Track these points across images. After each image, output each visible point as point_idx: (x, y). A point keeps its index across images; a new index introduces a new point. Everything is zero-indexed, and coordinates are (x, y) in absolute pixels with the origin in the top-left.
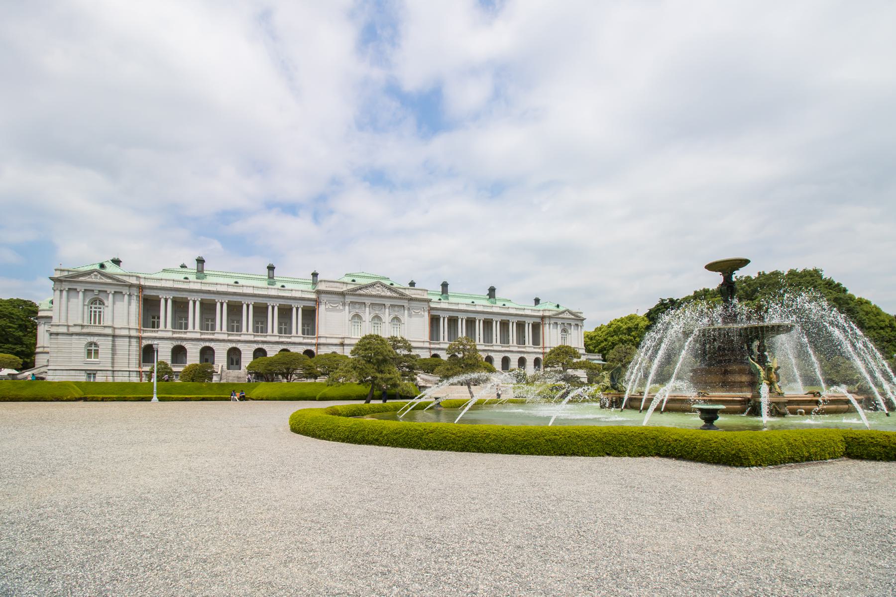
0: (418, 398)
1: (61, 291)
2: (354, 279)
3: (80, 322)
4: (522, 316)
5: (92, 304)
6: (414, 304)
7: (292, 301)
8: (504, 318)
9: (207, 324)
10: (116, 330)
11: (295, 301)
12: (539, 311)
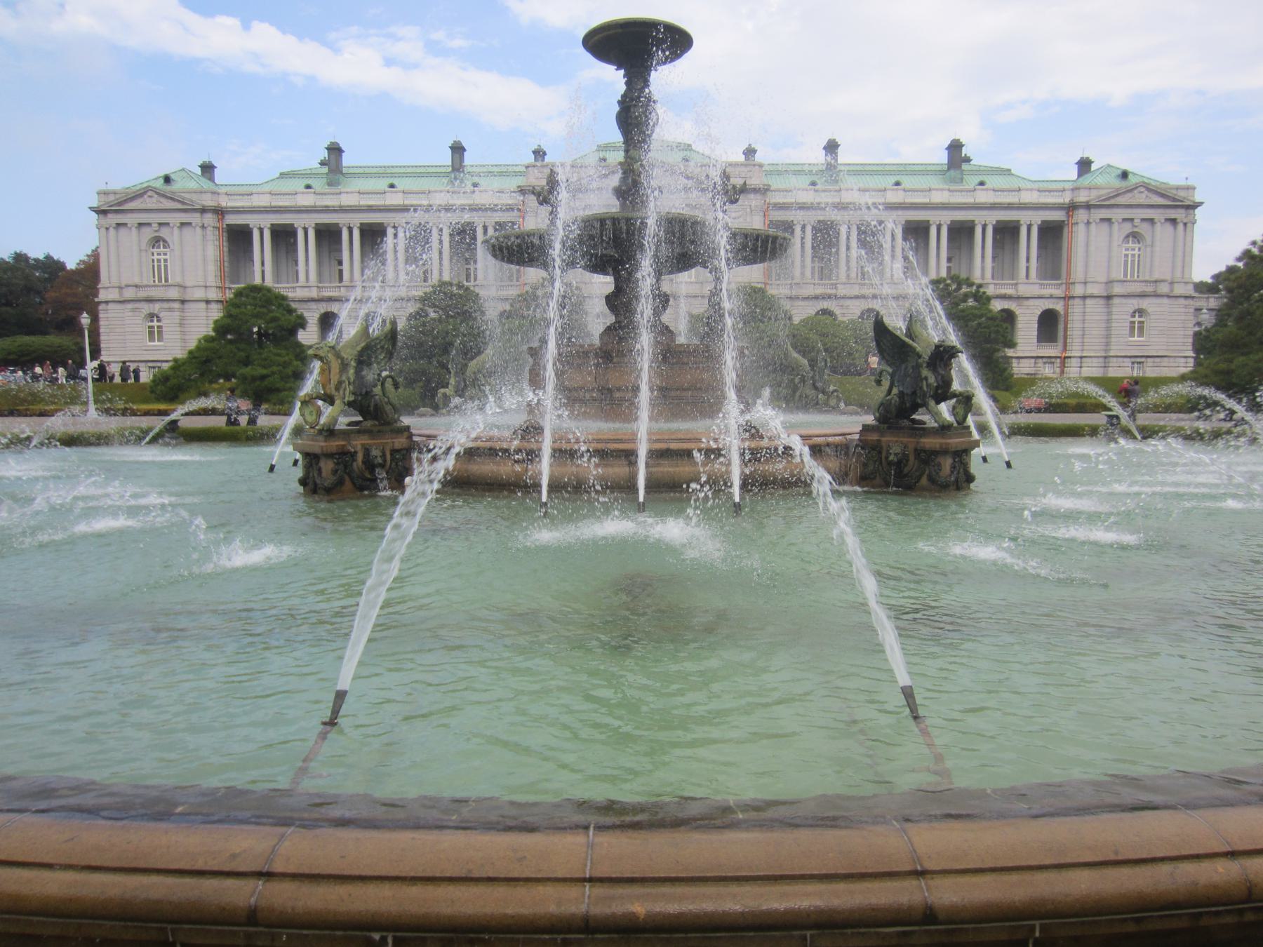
1: (107, 229)
3: (137, 281)
4: (1009, 207)
5: (153, 248)
10: (188, 290)
12: (1064, 190)
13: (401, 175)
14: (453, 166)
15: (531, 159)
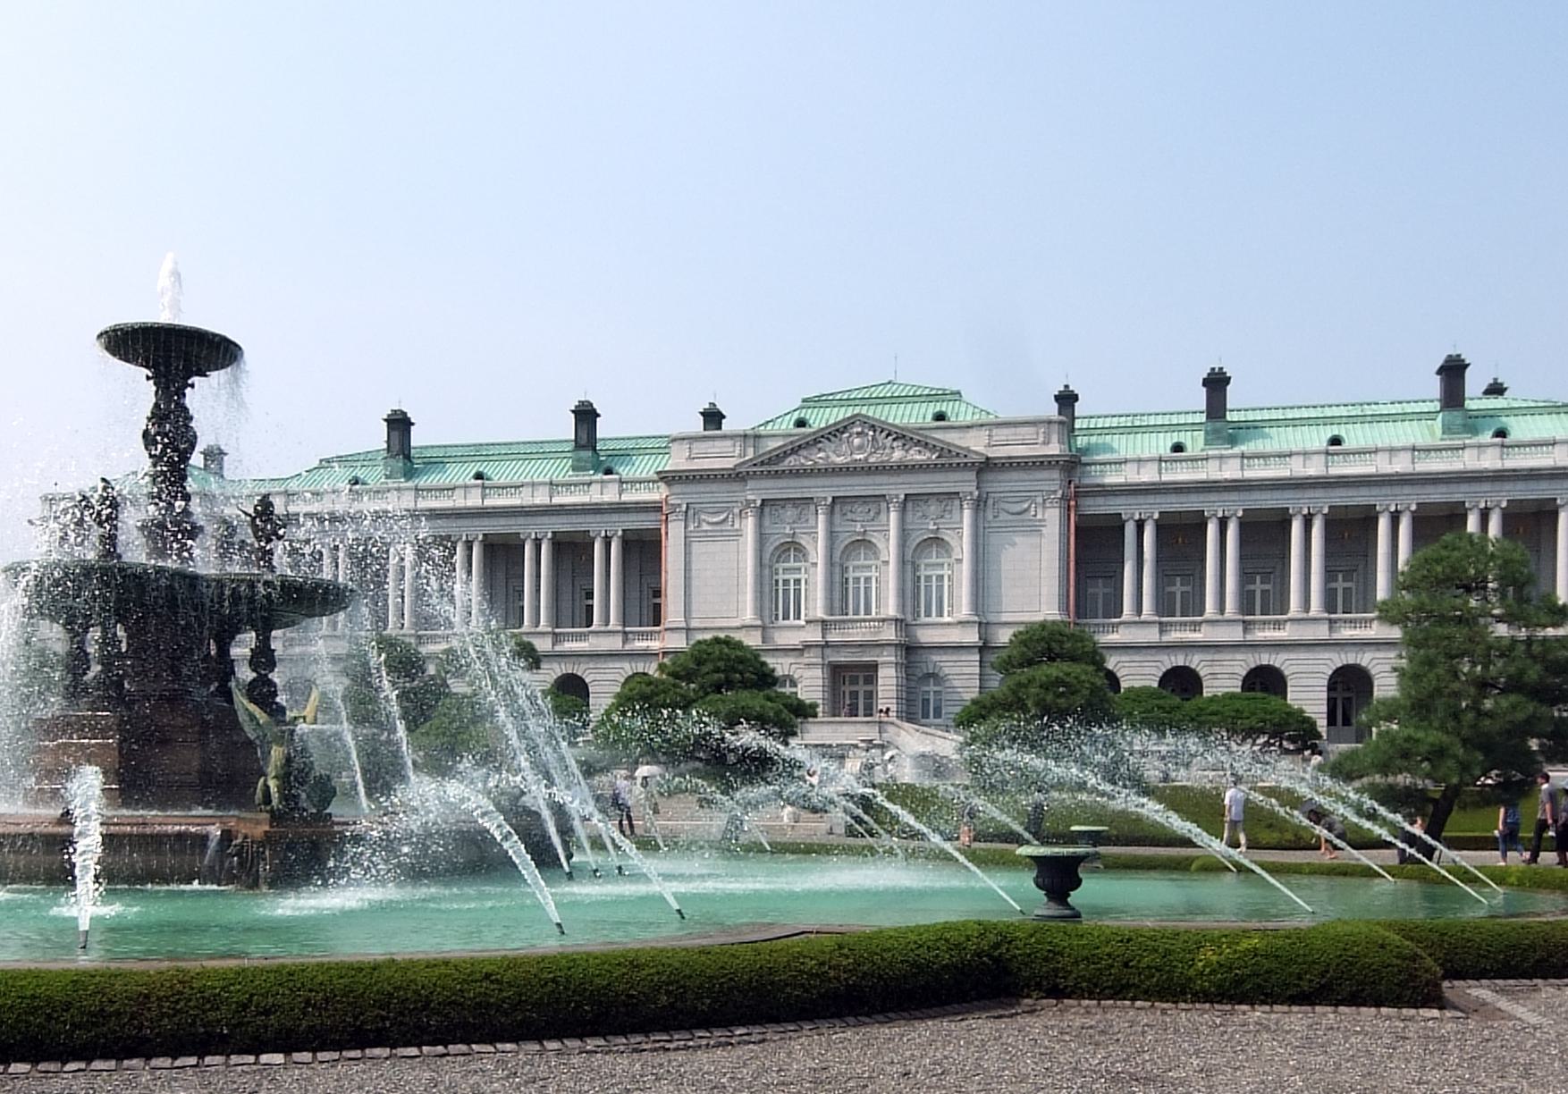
0: (1195, 846)
2: (943, 407)
6: (1001, 484)
7: (590, 518)
8: (1437, 495)
9: (655, 604)
11: (598, 518)
13: (488, 458)
14: (576, 440)
15: (697, 425)
